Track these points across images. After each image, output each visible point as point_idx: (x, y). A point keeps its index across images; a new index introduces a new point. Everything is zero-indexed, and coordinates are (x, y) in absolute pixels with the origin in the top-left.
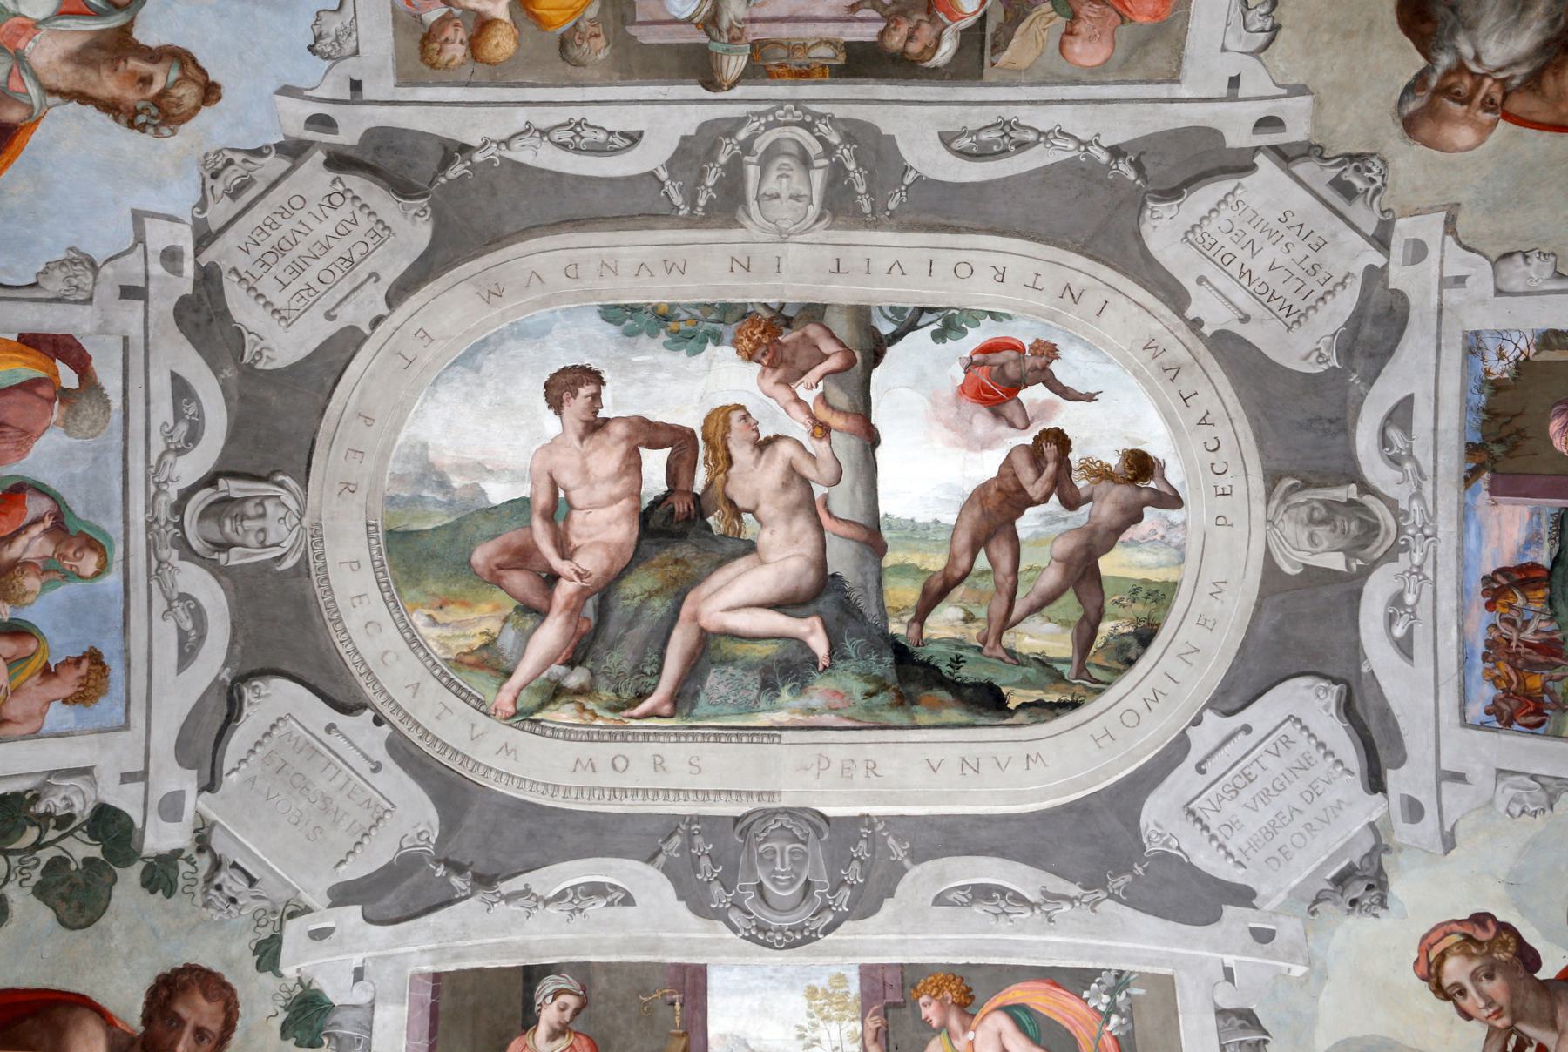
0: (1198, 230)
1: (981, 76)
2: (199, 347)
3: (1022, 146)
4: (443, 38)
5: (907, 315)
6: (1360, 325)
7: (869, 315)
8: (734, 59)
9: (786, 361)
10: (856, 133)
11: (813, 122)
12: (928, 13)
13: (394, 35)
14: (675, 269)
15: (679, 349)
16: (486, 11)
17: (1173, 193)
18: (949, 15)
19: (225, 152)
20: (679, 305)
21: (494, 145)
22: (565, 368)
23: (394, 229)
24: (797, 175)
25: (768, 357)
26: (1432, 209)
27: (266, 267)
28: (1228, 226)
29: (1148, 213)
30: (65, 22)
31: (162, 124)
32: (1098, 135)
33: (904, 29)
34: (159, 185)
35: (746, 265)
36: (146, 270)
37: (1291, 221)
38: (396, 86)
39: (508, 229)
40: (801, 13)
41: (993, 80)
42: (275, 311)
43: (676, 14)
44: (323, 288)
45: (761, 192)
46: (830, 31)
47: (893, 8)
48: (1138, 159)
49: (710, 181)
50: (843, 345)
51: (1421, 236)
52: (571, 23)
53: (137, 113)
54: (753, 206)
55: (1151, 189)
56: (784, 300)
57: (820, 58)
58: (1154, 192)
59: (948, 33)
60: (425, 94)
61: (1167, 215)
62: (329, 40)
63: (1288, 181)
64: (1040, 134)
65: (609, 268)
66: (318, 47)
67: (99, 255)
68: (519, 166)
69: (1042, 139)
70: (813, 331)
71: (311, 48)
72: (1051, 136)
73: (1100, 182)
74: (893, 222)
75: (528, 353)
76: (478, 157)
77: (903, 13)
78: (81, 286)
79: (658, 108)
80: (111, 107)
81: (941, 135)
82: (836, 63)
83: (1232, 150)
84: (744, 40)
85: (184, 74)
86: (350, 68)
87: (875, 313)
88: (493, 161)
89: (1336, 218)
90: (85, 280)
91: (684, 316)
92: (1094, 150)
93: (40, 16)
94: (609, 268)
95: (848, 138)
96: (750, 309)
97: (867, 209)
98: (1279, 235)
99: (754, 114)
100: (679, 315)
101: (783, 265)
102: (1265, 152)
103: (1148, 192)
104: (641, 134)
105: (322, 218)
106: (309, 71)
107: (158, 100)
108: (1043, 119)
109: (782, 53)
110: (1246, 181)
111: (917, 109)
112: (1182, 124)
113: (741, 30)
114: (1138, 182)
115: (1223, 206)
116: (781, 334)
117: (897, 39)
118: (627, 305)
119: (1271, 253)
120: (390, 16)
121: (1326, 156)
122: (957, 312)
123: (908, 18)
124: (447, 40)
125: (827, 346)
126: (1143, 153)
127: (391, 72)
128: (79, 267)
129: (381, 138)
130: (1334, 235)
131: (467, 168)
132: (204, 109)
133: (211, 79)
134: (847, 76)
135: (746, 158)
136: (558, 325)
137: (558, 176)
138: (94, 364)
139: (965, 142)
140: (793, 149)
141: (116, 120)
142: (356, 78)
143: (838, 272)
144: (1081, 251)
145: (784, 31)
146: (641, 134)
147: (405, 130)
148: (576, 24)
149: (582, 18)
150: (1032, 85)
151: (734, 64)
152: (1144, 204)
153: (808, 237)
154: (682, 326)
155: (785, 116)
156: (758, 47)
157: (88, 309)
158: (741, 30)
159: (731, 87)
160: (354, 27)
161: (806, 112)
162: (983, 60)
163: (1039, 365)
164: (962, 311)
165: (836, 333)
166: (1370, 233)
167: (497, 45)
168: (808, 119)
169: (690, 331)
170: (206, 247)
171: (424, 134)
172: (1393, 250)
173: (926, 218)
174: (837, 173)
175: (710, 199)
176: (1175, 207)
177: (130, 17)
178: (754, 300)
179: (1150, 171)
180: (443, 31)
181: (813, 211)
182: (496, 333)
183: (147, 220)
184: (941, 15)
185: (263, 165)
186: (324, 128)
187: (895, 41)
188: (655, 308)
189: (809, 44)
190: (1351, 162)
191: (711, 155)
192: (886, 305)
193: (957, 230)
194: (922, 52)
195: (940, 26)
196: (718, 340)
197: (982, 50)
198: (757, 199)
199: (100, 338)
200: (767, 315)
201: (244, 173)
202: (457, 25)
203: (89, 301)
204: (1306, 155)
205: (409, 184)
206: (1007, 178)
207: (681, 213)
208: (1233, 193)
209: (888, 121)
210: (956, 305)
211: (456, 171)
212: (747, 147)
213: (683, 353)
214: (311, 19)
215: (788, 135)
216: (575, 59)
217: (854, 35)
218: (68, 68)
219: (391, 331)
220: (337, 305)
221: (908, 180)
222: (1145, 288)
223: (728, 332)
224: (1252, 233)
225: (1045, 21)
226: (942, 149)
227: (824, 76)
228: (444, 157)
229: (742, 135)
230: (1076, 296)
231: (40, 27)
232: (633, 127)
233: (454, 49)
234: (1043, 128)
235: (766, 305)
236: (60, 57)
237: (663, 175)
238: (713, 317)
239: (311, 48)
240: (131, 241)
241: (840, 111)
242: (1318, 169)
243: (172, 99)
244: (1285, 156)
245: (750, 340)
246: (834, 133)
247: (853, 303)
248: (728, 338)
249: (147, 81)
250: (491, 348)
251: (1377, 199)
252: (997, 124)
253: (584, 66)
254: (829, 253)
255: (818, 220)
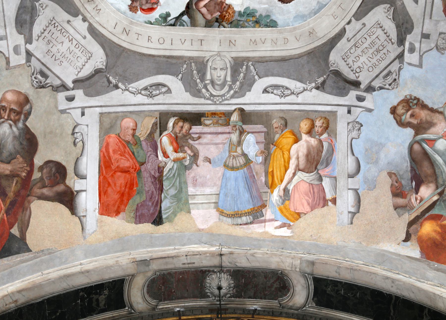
0: (88, 58)
1: (160, 114)
2: (407, 14)
3: (146, 89)
4: (322, 128)
5: (179, 23)
6: (31, 20)
7: (191, 23)
8: (235, 120)
9: (217, 5)
10: (197, 93)
11: (210, 97)
12: (177, 136)
13: (337, 129)
14: (253, 41)
15: (252, 10)
16: (309, 137)
17: (97, 72)
18: (171, 136)
19: (391, 88)
20: (252, 27)
21: (308, 89)
22: (290, 3)
23: (341, 58)
24: (215, 77)
25: (223, 6)
26: (15, 67)
27: (383, 45)
28: (79, 59)
29: (104, 64)
30: (434, 138)
31: (409, 100)
32: (123, 93)
33: (184, 130)
34: (413, 77)
35: (231, 43)
36: (420, 45)
37: (58, 62)
38: (337, 111)
39: (305, 58)
40: (215, 136)
41: (156, 113)
42: (381, 27)
43: (252, 135)
44: (365, 36)
45: (226, 71)
46: (206, 130)
47: (188, 138)
48: (109, 85)
49: (242, 75)
50: (199, 11)
51: (16, 56)
52: (284, 132)
53: (416, 104)
54: (228, 66)
55: (104, 73)
56: (219, 29)
57: (209, 120)
58: (103, 72)
59: (171, 129)
60: (328, 108)
61: (98, 63)
62: (356, 128)
63: (61, 77)
64: (140, 93)
65: (274, 42)
66: (360, 126)
67: (435, 51)
68: (301, 81)
69: (140, 91)
70: (209, 17)
71: (362, 126)
72: (137, 92)
73: (120, 76)
74: (184, 59)
75: (302, 9)
76: (313, 85)
77: (185, 136)
78: (442, 40)
79: (258, 102)
80: (424, 106)
81: (171, 93)
82: (204, 118)
83: (81, 89)
84: (232, 126)
85: (401, 117)
86: (351, 118)
87: (189, 24)
88: (309, 83)
89: (44, 63)
90: (440, 41)
91: (250, 23)
92: (123, 87)
93: (441, 140)
94: (274, 42)
95: (199, 91)
96: (229, 25)
97: (193, 64)
98: (62, 56)
99: (228, 100)
100: (252, 23)
101: (219, 43)
102: (71, 88)
103: (105, 72)
104: (263, 93)
105: (363, 63)
106: (363, 117)
107: (409, 108)
108: (140, 99)
109: (220, 122)
110: (75, 77)
111: (179, 102)
112: (97, 98)
113: (233, 130)
114: (108, 76)
115: (81, 67)
116: (219, 16)
117: (186, 127)
118: (269, 27)
119: (63, 48)
120: (337, 136)
121: (51, 87)
122: (163, 24)
123: (183, 134)
124: (321, 127)
125: (204, 10)
126: (108, 87)
127: (338, 117)
128: (441, 47)
129: (342, 93)
130: (44, 56)
131: (317, 81)
132: (396, 104)
133: (393, 116)
134: (200, 113)
135: (231, 83)
136: (291, 20)
137: (289, 77)
138: (442, 9)
139: (164, 90)
140: (217, 87)
141: (423, 102)
142: (349, 114)
143: (201, 40)
144: (125, 48)
145: (220, 129)
146: (263, 93)
147: (335, 95)
148: (282, 132)
149: (280, 134)
150: (144, 111)
151: (235, 117)
152: (106, 68)
153: (211, 54)
154: (251, 19)
155: (219, 99)
156: (227, 124)
157: (441, 30)
158: (233, 130)
159: (236, 109)
160: (348, 133)
161: (212, 100)
162: (160, 120)
163: (135, 3)
164: (161, 25)
165: (202, 16)
166: (33, 58)
167: (306, 125)
168: (212, 98)
169: (249, 17)
170: (401, 53)
171: (329, 94)
172: (24, 51)
173: (174, 61)
174: (203, 78)
175: (242, 68)
176: (96, 66)
177: (415, 138)
178: (228, 29)
179: (105, 80)
180: (322, 130)
181: (210, 64)
182: (312, 17)
183: (418, 64)
184: (173, 135)
185: (380, 83)
186: (360, 97)
187: (186, 126)
188: (260, 27)
189: (212, 125)
190: (43, 85)
191: (242, 84)
192: (186, 27)
193: (164, 56)
194: (178, 122)
195: (173, 132)
196: (240, 14)
197: (160, 123)
198: (227, 68)
199: (439, 19)
200: (224, 23)
201: (386, 81)
202: (318, 132)
203: (440, 34)
204: (57, 87)
205: (336, 76)
206: (149, 76)
207: (251, 63)
208: (79, 72)
209: (187, 97)
210: (163, 27)
211: (320, 80)
212: (231, 88)
213: (251, 8)
214: (361, 135)
215: (218, 92)
216: (283, 120)
217: (199, 128)
218: (435, 121)
219: (345, 19)
220: (361, 29)
221: (180, 75)
222: (102, 34)
223: (236, 17)
224: (70, 56)
225: (142, 134)
226: (170, 87)
227: (207, 113)
228: (324, 85)
229: (232, 92)
230: (124, 31)
231: (441, 136)
232: (266, 95)
233: (319, 124)
234: (139, 95)
235: (224, 27)
236: (437, 125)
237: (256, 77)
238: (241, 23)
239: (362, 126)
240: (424, 56)
241: (202, 101)
242: (53, 82)
243: (405, 108)
244: (64, 87)
245: (229, 13)
246: (204, 93)
247: (196, 28)
248: (237, 14)
249: (412, 116)
250: (313, 11)
251: (33, 71)
252: (154, 96)
253: (280, 117)
254: (205, 48)
255: (208, 60)
